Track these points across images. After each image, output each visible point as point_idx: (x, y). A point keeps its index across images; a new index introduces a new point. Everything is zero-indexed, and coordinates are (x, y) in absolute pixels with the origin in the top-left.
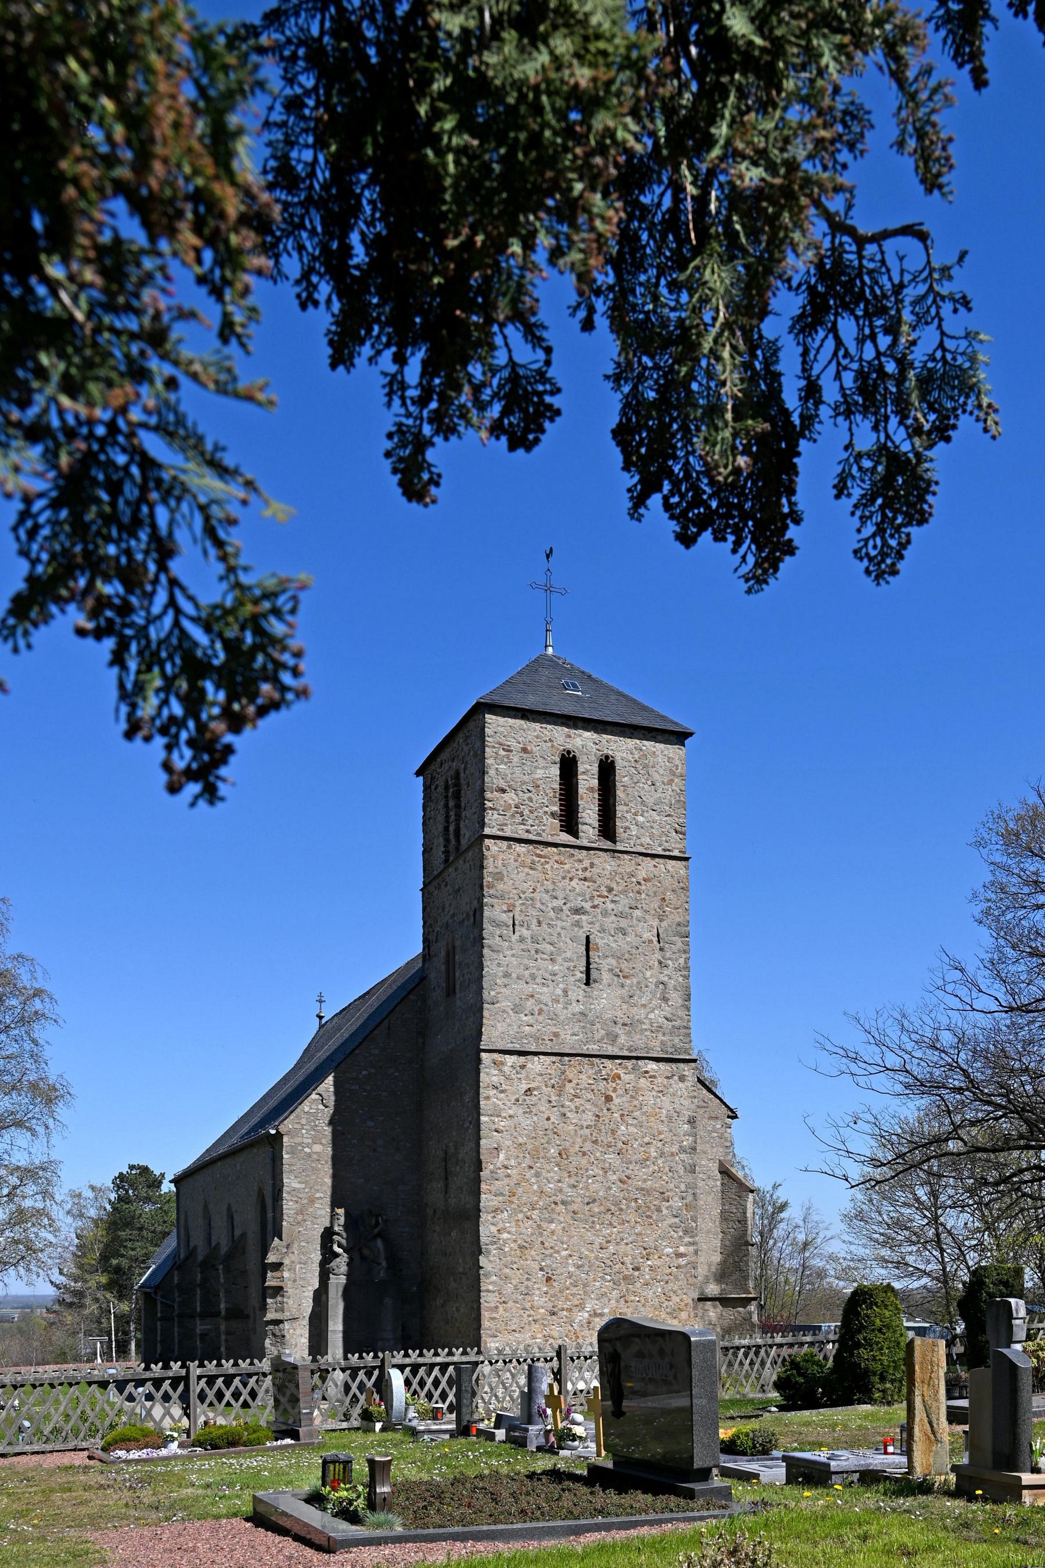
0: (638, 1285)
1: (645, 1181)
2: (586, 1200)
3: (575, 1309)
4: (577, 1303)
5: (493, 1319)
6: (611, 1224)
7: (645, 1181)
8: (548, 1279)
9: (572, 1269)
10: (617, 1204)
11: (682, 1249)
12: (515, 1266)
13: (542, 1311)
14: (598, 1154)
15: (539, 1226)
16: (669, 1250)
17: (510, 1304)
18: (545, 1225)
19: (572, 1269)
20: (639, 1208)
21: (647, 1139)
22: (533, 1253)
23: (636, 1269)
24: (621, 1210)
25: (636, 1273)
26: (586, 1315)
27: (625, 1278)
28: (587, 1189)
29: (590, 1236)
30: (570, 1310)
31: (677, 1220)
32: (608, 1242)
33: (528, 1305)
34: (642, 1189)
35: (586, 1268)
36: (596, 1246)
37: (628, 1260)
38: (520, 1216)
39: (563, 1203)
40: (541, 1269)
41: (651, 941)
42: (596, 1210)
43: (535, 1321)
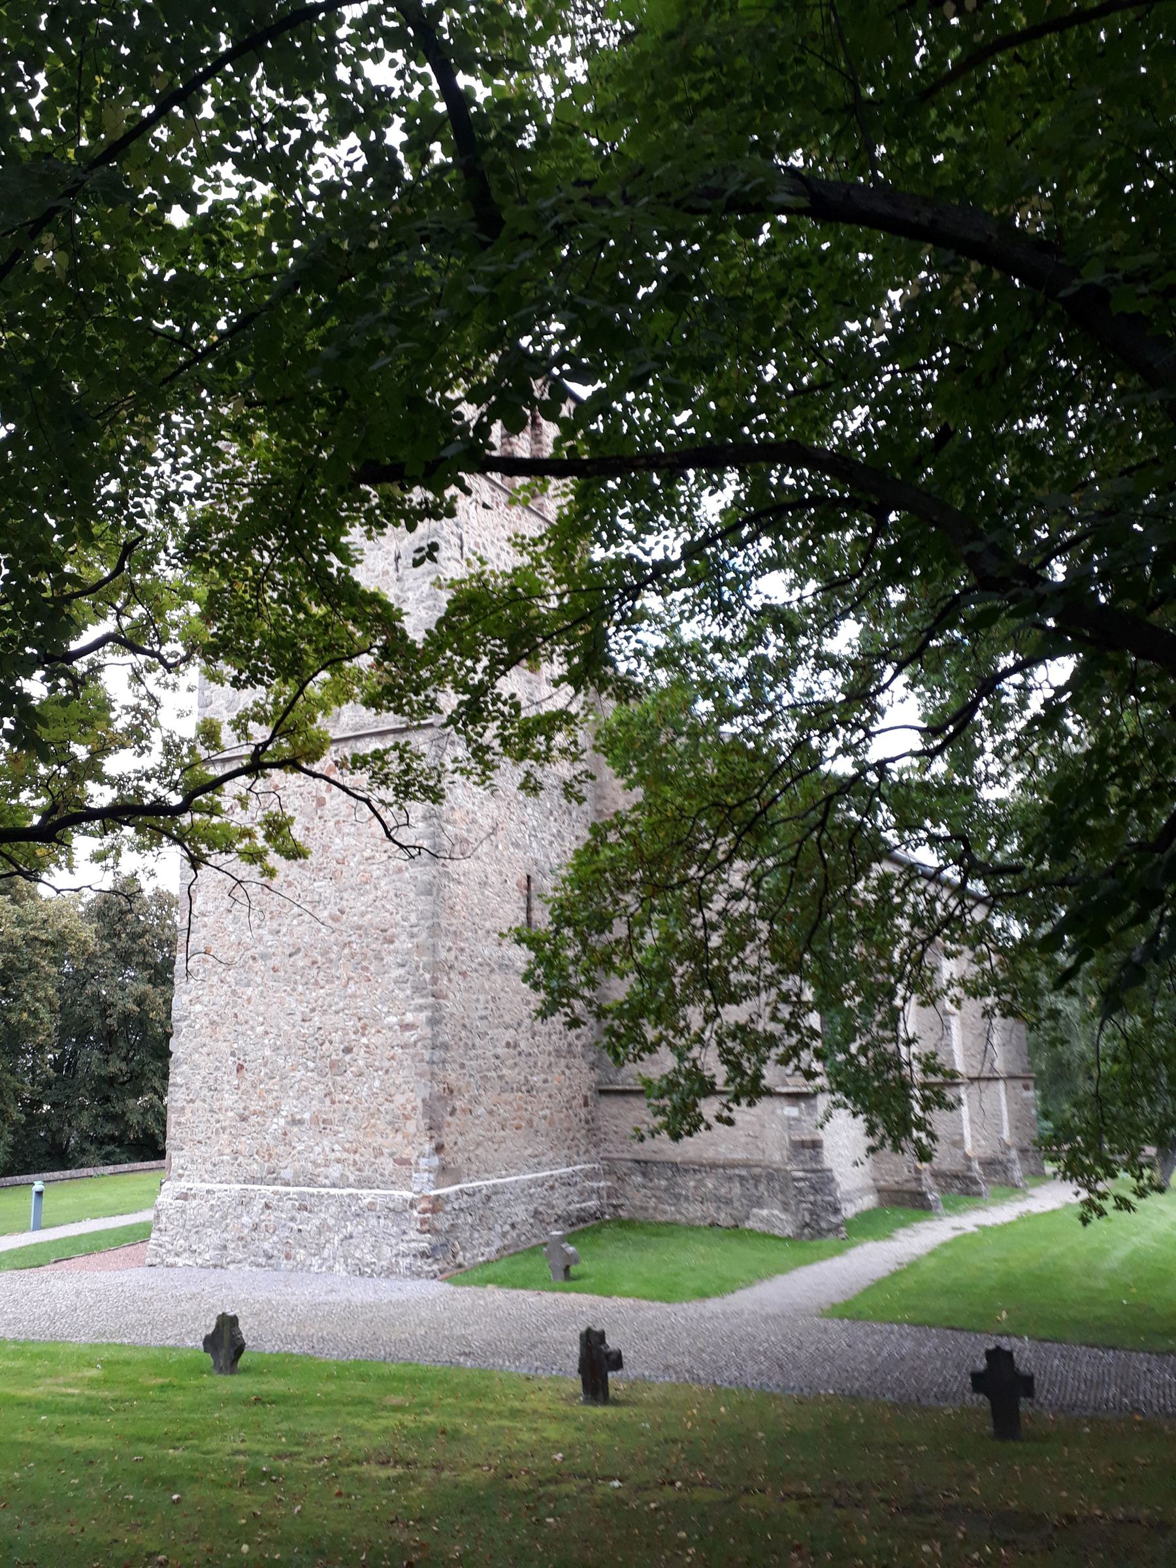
0: (349, 1074)
1: (363, 914)
2: (292, 950)
3: (270, 1113)
4: (271, 1103)
5: (179, 1124)
6: (316, 983)
7: (363, 914)
8: (240, 1068)
9: (268, 1053)
10: (324, 953)
11: (409, 1018)
12: (205, 1050)
13: (230, 1114)
14: (306, 883)
15: (234, 992)
16: (392, 1019)
17: (198, 1103)
18: (239, 990)
19: (268, 1053)
20: (353, 956)
21: (368, 853)
22: (225, 1030)
23: (348, 1050)
24: (331, 961)
25: (348, 1058)
26: (282, 1122)
27: (333, 1065)
28: (292, 934)
29: (291, 1003)
30: (262, 1114)
31: (401, 971)
32: (313, 1010)
33: (216, 1106)
34: (359, 928)
35: (284, 1051)
36: (298, 1017)
37: (336, 1037)
38: (215, 979)
39: (264, 957)
40: (233, 1054)
41: (386, 573)
42: (301, 964)
43: (224, 1129)
